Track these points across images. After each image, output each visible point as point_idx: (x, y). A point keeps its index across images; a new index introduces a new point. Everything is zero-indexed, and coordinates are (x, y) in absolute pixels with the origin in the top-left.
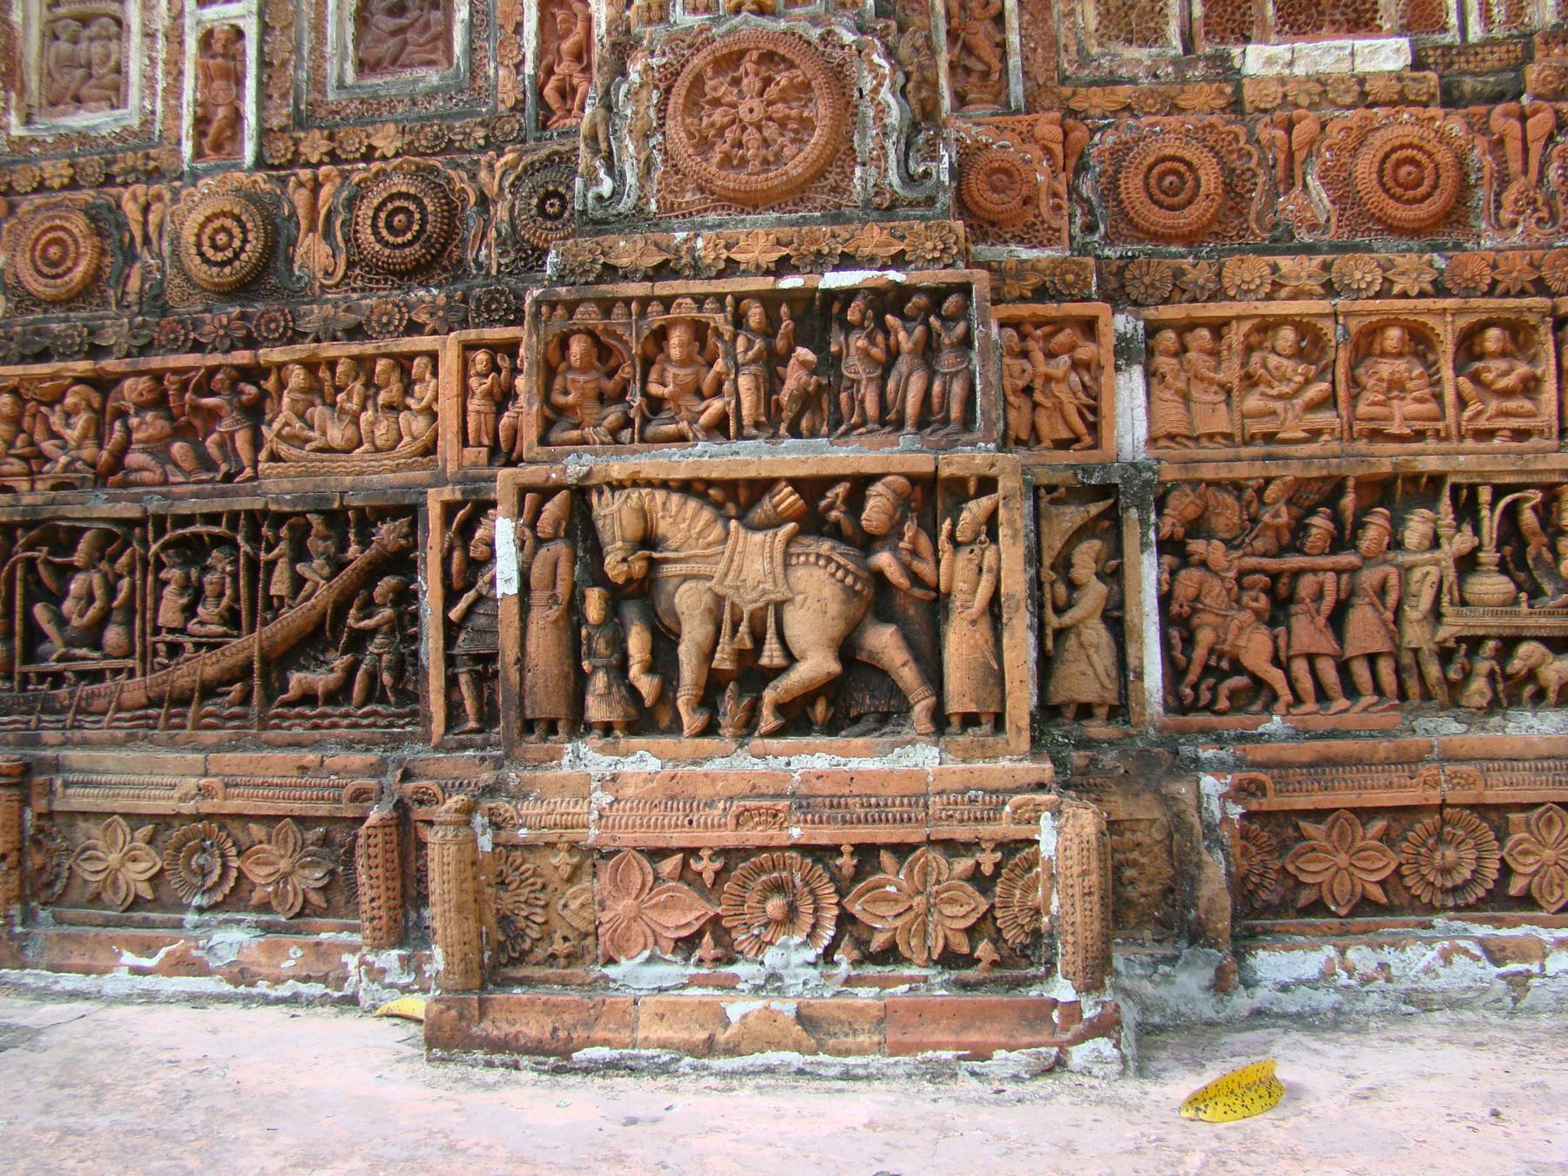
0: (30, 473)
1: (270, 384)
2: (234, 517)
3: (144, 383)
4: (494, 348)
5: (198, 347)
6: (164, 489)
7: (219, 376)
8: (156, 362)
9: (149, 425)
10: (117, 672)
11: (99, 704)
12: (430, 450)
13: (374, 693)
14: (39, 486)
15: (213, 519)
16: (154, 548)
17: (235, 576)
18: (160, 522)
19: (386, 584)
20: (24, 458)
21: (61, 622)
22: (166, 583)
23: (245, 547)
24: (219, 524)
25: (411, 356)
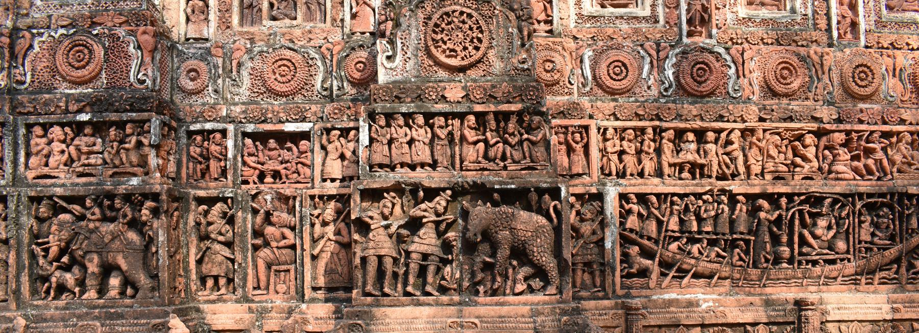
0: (789, 171)
1: (894, 139)
2: (892, 195)
5: (861, 122)
6: (855, 182)
7: (875, 135)
8: (848, 127)
9: (844, 154)
10: (842, 260)
11: (834, 274)
14: (796, 177)
16: (858, 207)
17: (893, 220)
20: (786, 165)
21: (815, 237)
22: (864, 222)
24: (885, 198)
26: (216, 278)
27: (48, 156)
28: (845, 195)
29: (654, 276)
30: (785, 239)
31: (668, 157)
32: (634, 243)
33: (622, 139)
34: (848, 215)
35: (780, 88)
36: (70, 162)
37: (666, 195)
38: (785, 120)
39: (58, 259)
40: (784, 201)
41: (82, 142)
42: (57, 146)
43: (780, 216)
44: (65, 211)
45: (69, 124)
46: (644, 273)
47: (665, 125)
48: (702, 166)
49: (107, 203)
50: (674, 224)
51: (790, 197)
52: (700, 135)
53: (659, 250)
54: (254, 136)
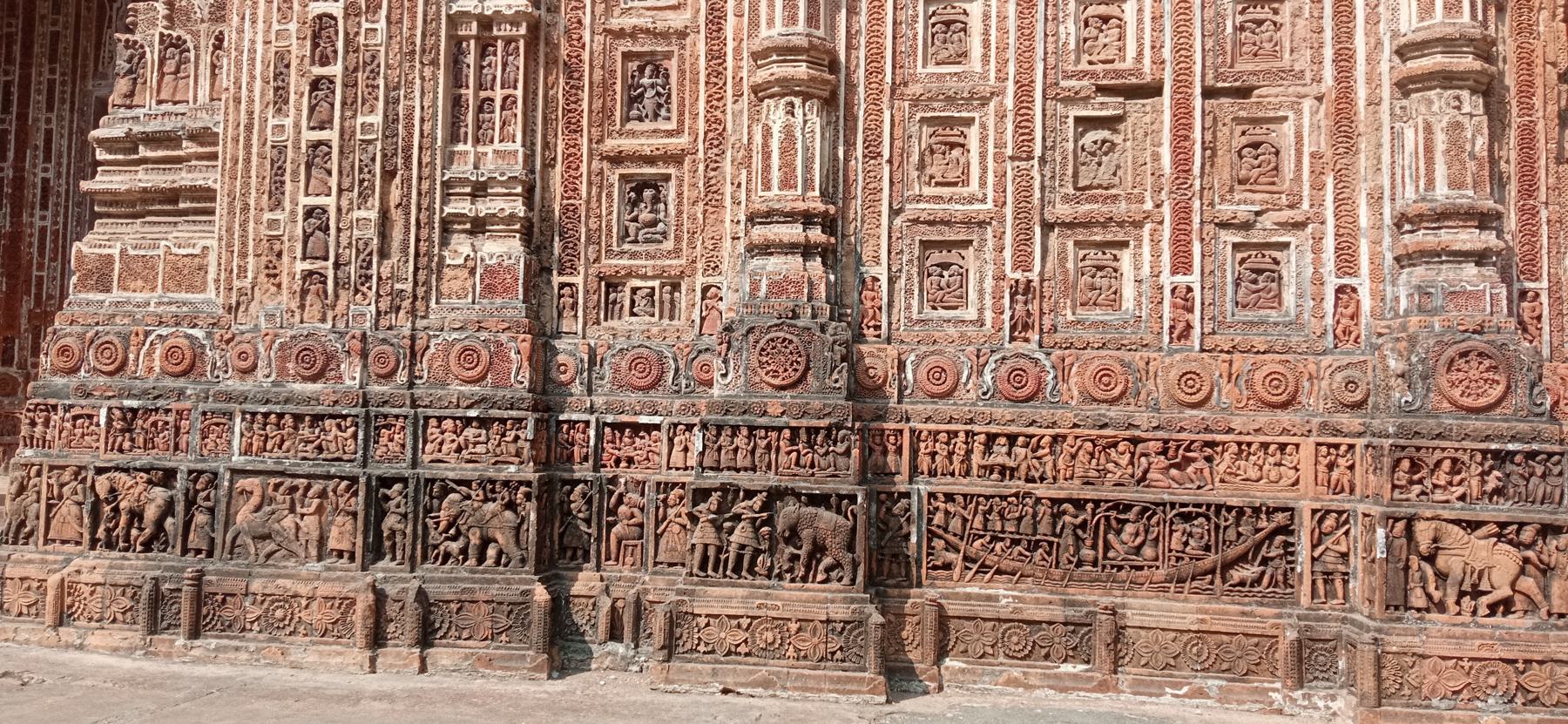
1: (1219, 449)
2: (1209, 506)
3: (1160, 444)
4: (1329, 446)
11: (1141, 580)
12: (1296, 482)
13: (1273, 582)
15: (1199, 506)
18: (1173, 505)
19: (1279, 539)
23: (1214, 519)
25: (1286, 445)
26: (575, 550)
27: (441, 444)
28: (1157, 505)
29: (957, 570)
30: (1089, 542)
31: (976, 459)
32: (940, 537)
33: (936, 441)
34: (1158, 524)
35: (1099, 395)
36: (459, 450)
37: (972, 496)
38: (1101, 427)
39: (446, 531)
40: (1090, 506)
41: (470, 432)
42: (449, 436)
43: (1085, 521)
44: (454, 491)
45: (460, 418)
46: (948, 566)
47: (976, 428)
48: (1013, 470)
49: (489, 487)
50: (978, 522)
51: (1097, 503)
52: (1012, 439)
53: (962, 545)
54: (614, 426)
